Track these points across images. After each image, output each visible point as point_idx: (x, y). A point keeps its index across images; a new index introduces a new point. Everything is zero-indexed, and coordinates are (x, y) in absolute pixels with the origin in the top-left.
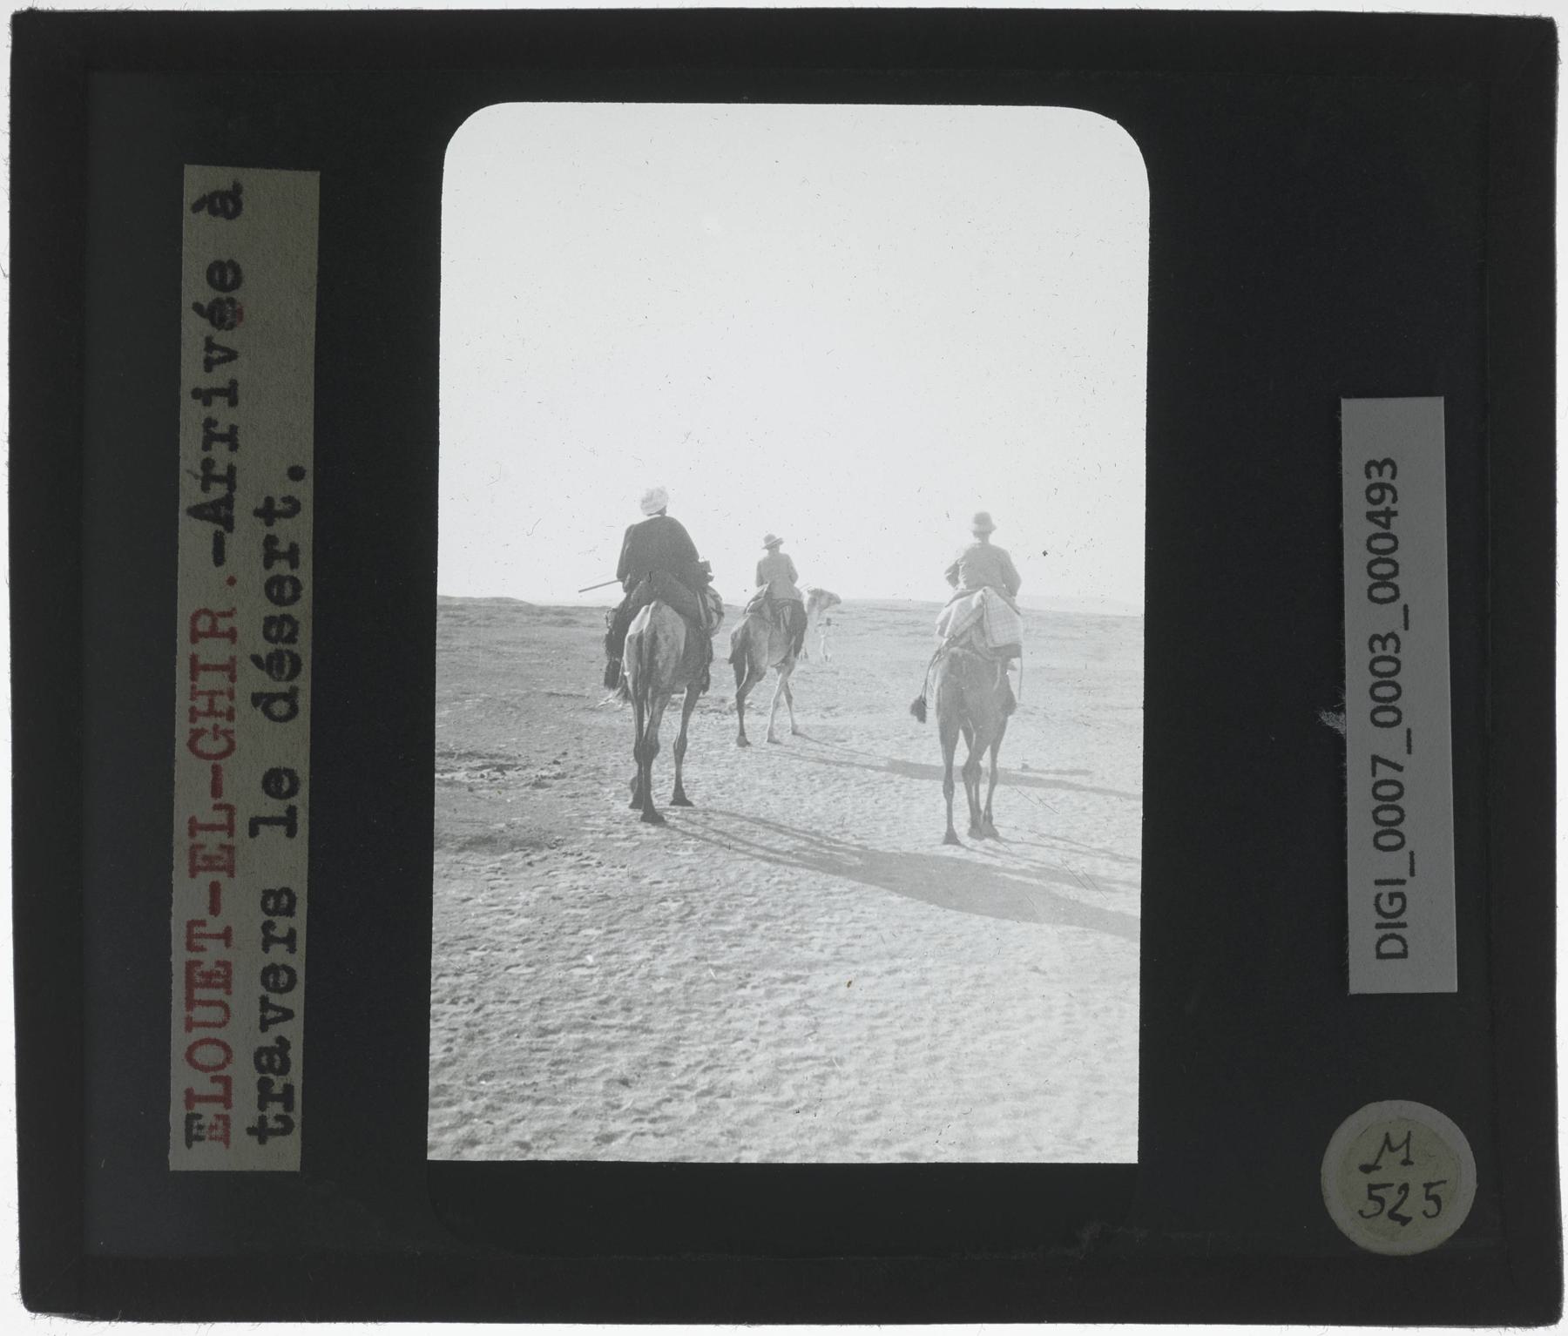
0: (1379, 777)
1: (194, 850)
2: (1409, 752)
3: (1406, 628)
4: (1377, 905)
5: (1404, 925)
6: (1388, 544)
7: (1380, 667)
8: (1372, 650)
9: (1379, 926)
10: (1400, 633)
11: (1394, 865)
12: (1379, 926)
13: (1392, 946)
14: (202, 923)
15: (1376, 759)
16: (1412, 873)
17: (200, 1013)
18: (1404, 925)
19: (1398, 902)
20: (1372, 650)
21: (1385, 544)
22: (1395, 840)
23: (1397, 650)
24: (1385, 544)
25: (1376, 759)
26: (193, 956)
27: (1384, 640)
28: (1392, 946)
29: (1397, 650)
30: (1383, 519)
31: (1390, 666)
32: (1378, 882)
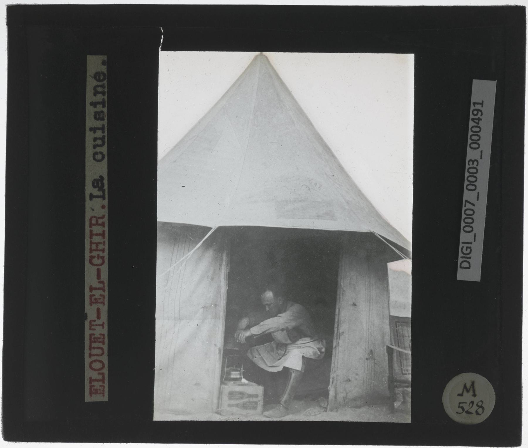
0: (467, 208)
1: (91, 296)
2: (478, 200)
3: (481, 158)
5: (470, 258)
6: (478, 129)
8: (469, 165)
10: (479, 160)
13: (465, 265)
14: (95, 321)
16: (475, 241)
17: (94, 352)
19: (469, 250)
21: (477, 129)
23: (477, 165)
24: (477, 129)
25: (466, 201)
26: (92, 332)
27: (473, 161)
28: (465, 265)
29: (477, 165)
30: (477, 121)
31: (474, 171)
32: (463, 243)
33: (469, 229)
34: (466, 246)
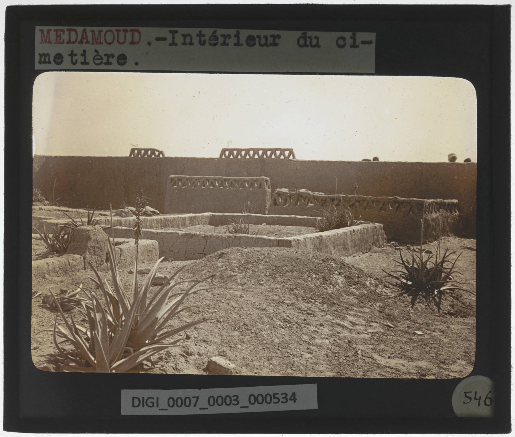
0: (191, 398)
2: (200, 409)
3: (241, 407)
4: (149, 398)
5: (143, 406)
7: (228, 399)
8: (233, 396)
9: (143, 398)
11: (163, 404)
12: (143, 398)
13: (136, 402)
15: (198, 398)
16: (160, 410)
17: (122, 34)
18: (143, 406)
19: (151, 405)
20: (233, 396)
22: (171, 404)
23: (234, 404)
25: (198, 398)
28: (136, 402)
29: (234, 404)
32: (158, 398)
33: (171, 404)
34: (155, 401)
